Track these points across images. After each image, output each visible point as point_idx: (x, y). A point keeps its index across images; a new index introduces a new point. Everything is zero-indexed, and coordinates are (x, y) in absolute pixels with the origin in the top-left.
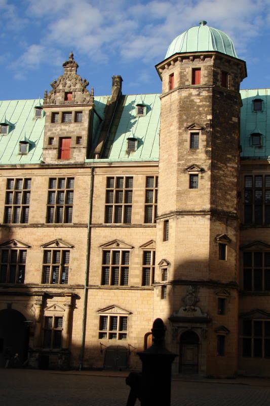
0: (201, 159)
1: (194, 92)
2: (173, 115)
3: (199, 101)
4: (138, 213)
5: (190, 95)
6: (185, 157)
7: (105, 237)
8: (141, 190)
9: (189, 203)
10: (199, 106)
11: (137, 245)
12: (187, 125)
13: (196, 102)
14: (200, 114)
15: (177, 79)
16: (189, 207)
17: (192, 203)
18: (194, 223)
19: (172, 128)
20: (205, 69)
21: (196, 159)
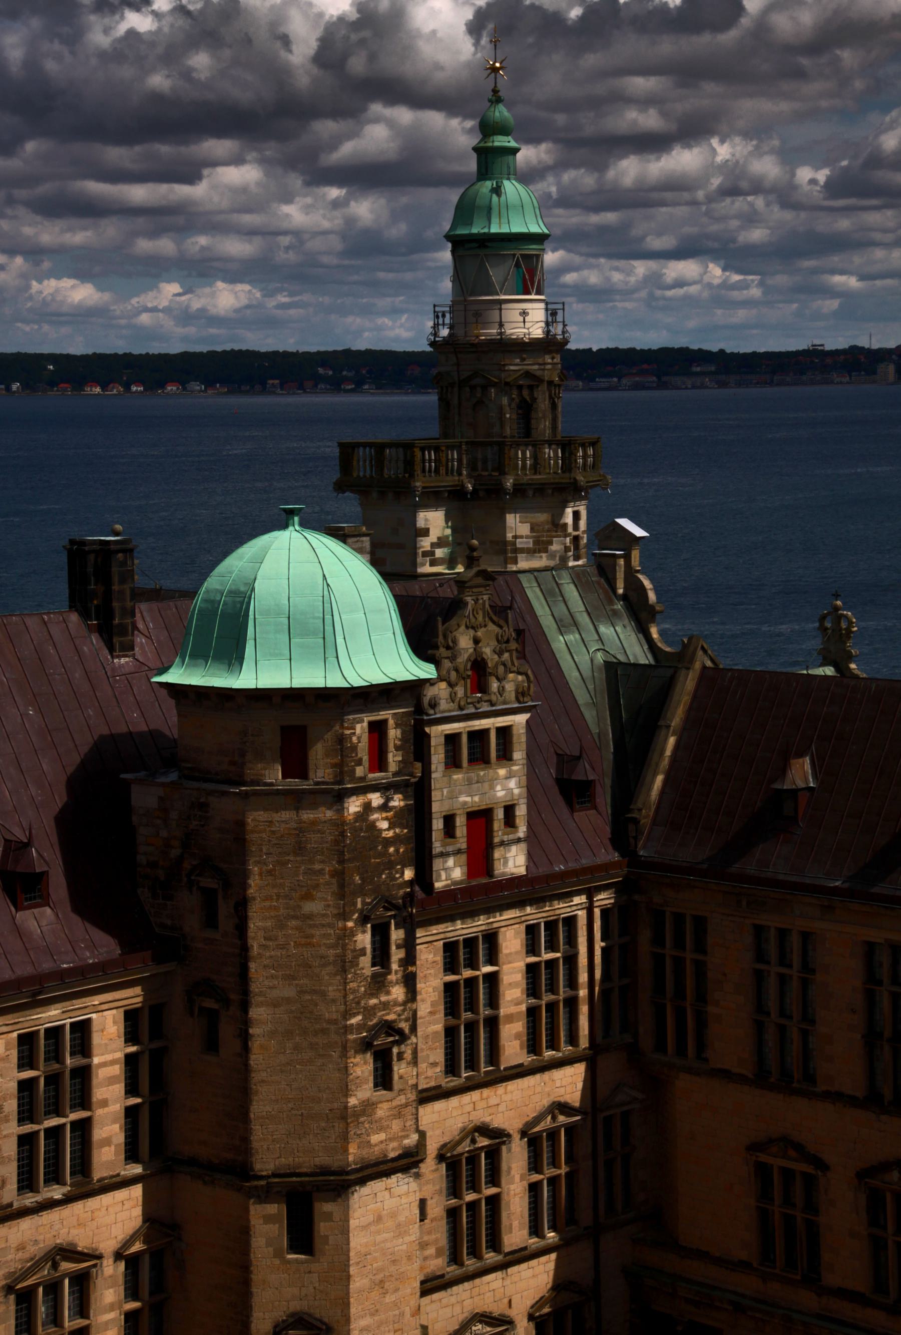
0: (396, 1003)
1: (376, 799)
2: (317, 867)
3: (384, 825)
4: (107, 1142)
5: (367, 807)
6: (363, 1003)
7: (21, 1247)
8: (113, 1062)
9: (375, 1138)
10: (388, 842)
11: (108, 1245)
12: (363, 903)
13: (381, 831)
14: (390, 865)
15: (327, 755)
16: (376, 1149)
17: (382, 1136)
18: (387, 1193)
19: (309, 907)
20: (397, 726)
21: (385, 1006)
